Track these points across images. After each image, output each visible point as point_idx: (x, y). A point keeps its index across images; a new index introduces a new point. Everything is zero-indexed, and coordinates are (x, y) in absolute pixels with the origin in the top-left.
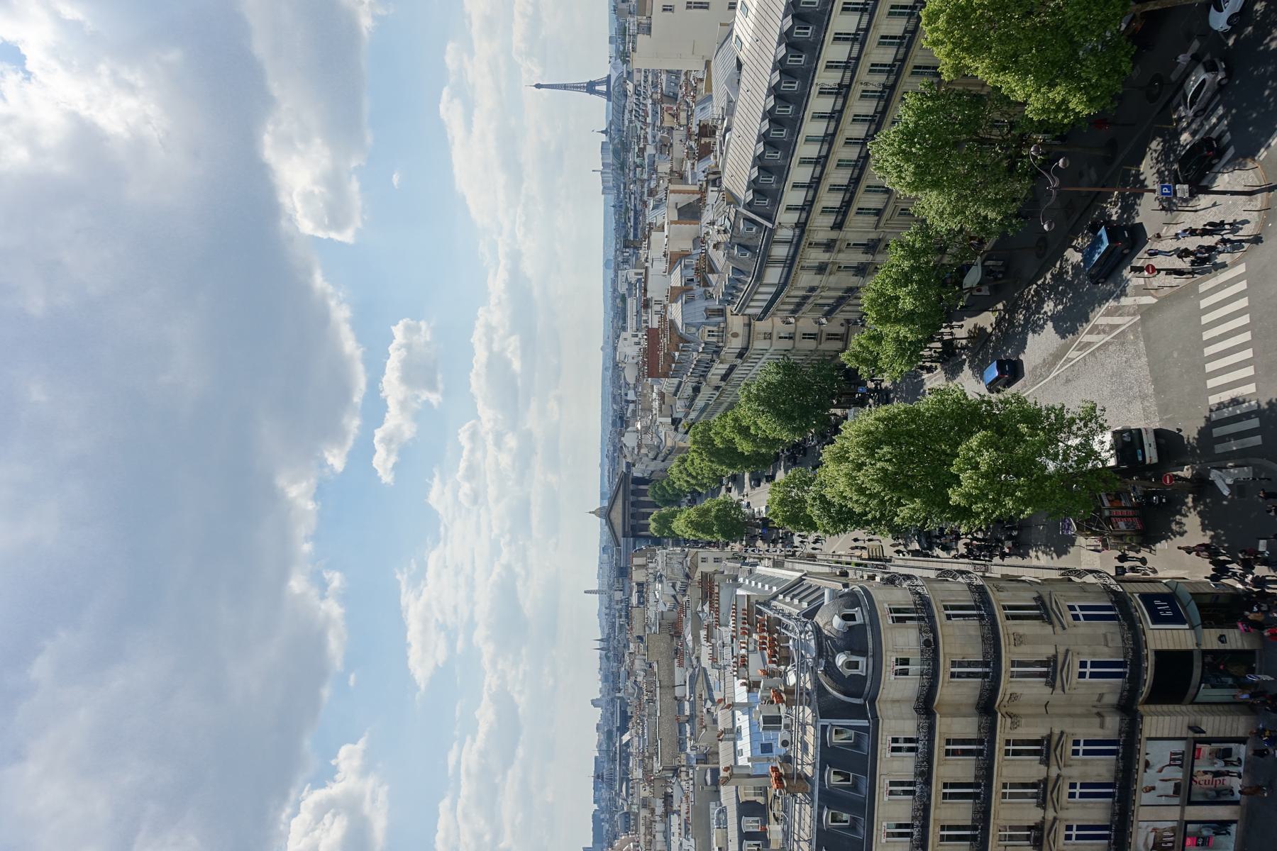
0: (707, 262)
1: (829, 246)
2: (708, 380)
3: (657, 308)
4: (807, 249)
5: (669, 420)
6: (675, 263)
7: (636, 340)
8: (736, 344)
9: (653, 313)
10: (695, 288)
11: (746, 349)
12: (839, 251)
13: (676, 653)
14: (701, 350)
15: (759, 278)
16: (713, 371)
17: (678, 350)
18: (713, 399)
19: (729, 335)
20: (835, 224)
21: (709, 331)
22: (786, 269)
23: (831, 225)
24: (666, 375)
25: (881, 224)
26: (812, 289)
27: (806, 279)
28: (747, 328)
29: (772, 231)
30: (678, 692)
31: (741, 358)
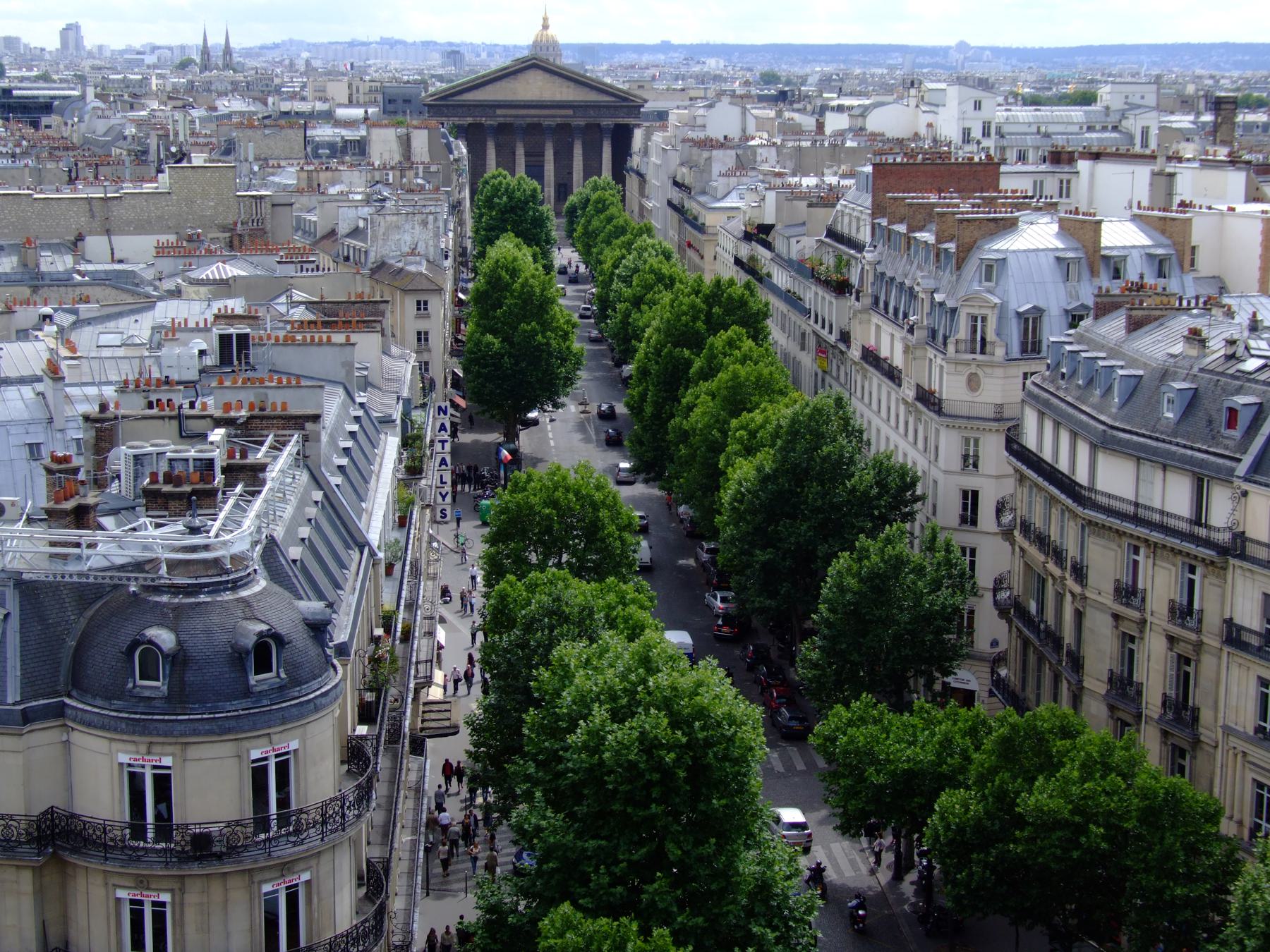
0: (1157, 313)
1: (1184, 612)
2: (865, 316)
3: (1051, 186)
4: (1179, 560)
5: (769, 220)
6: (1163, 232)
7: (977, 133)
8: (951, 388)
9: (1039, 178)
10: (1097, 282)
11: (939, 412)
12: (1172, 639)
13: (190, 239)
14: (938, 297)
15: (1104, 443)
16: (887, 328)
17: (939, 240)
18: (818, 327)
19: (973, 369)
20: (1240, 628)
21: (984, 319)
22: (1130, 509)
23: (1237, 621)
24: (878, 209)
25: (1233, 741)
26: (1079, 573)
29: (1226, 477)
30: (95, 244)
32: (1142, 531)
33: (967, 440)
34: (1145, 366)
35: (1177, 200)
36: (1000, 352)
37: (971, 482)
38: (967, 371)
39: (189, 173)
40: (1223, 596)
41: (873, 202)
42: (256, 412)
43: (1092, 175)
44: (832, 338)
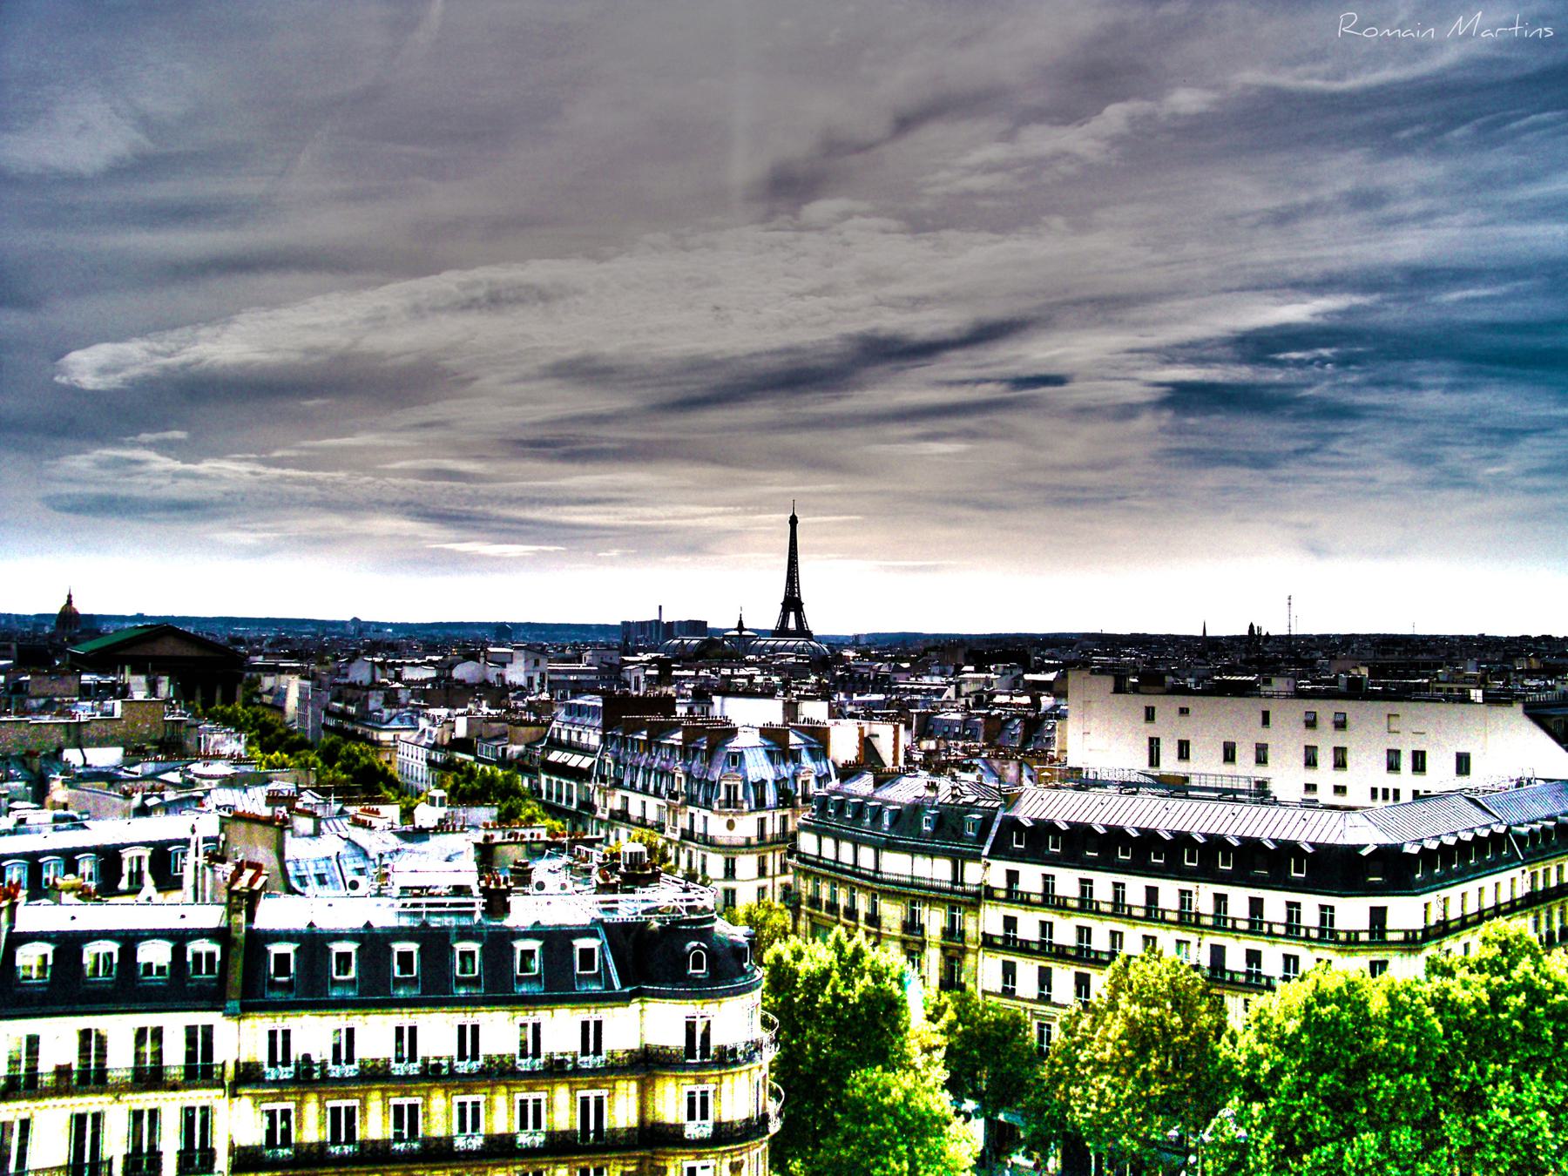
8: (716, 826)
10: (788, 764)
12: (944, 949)
19: (730, 817)
20: (992, 936)
21: (736, 787)
22: (909, 880)
23: (987, 932)
24: (605, 727)
27: (892, 914)
28: (743, 841)
29: (976, 857)
31: (683, 836)
32: (916, 891)
33: (727, 860)
34: (899, 804)
35: (801, 718)
36: (746, 806)
37: (730, 884)
38: (725, 819)
39: (134, 706)
40: (978, 921)
41: (604, 721)
42: (535, 839)
43: (722, 705)
44: (574, 806)
